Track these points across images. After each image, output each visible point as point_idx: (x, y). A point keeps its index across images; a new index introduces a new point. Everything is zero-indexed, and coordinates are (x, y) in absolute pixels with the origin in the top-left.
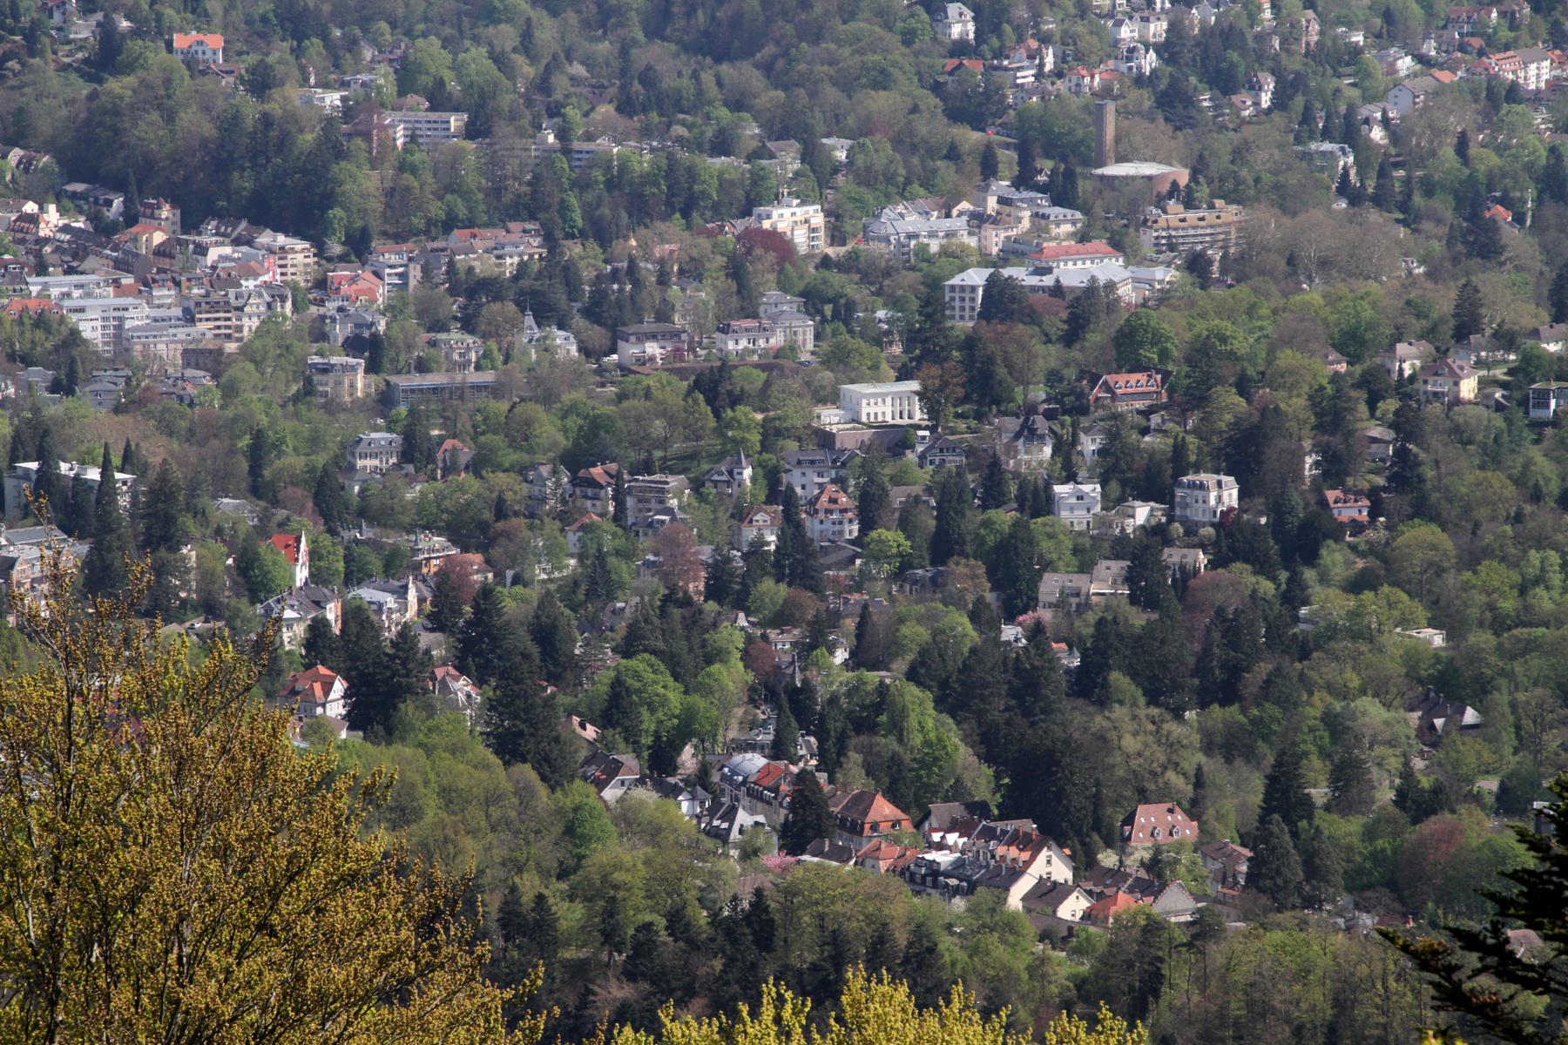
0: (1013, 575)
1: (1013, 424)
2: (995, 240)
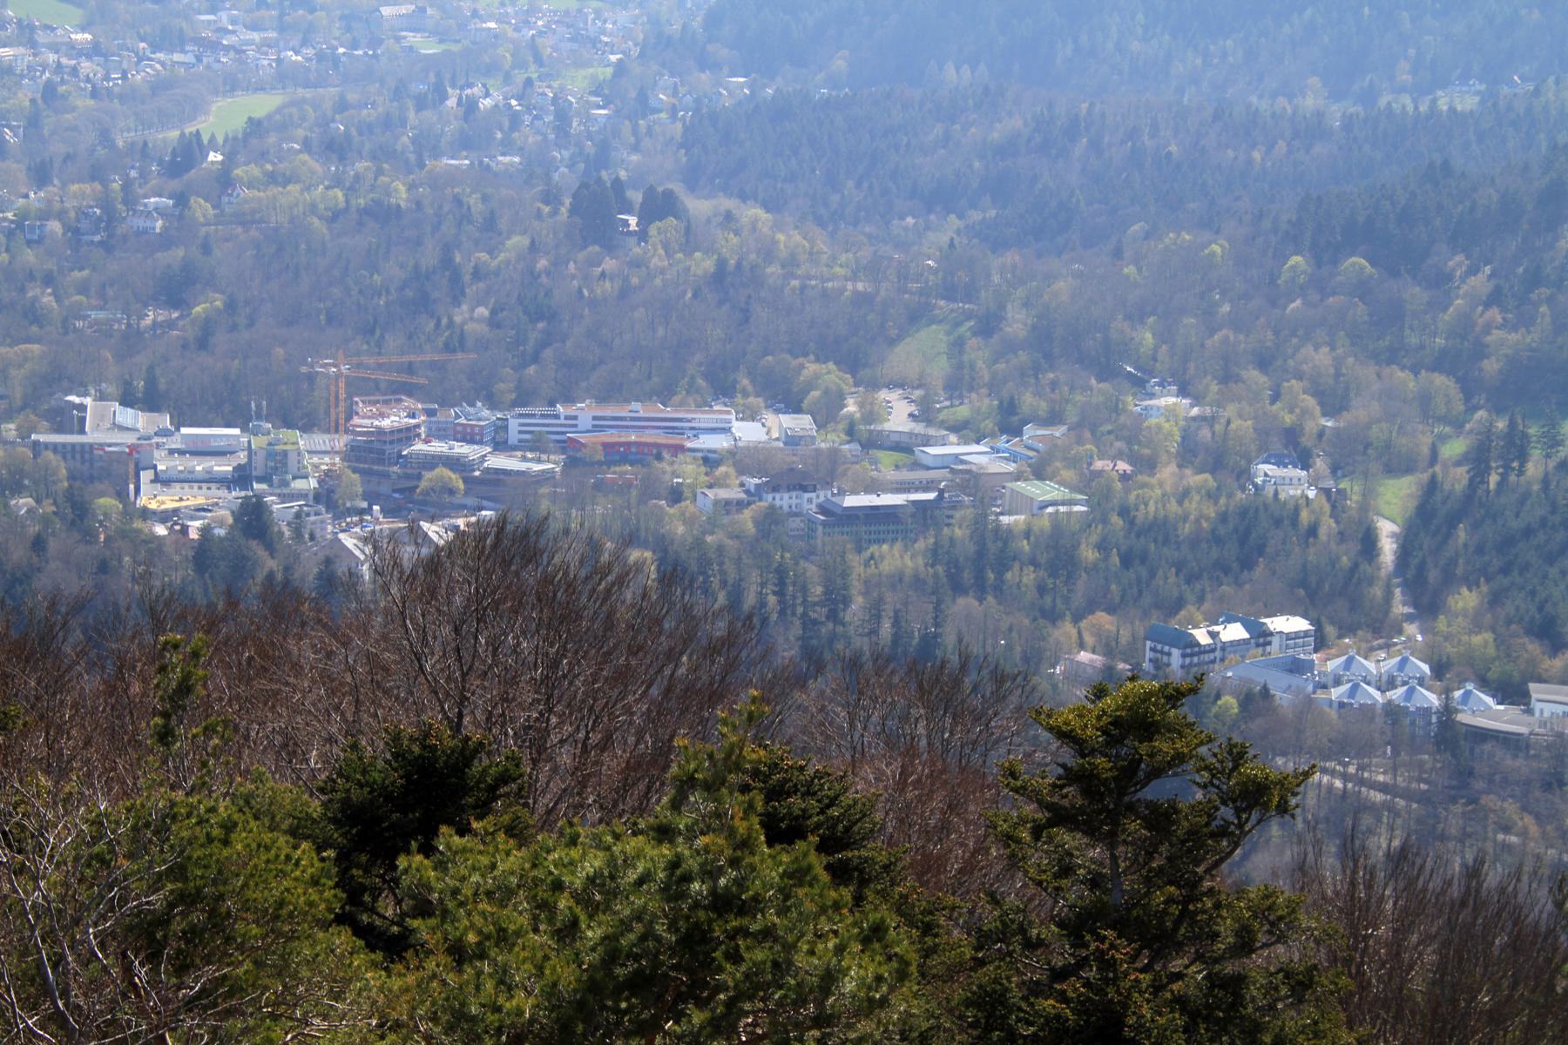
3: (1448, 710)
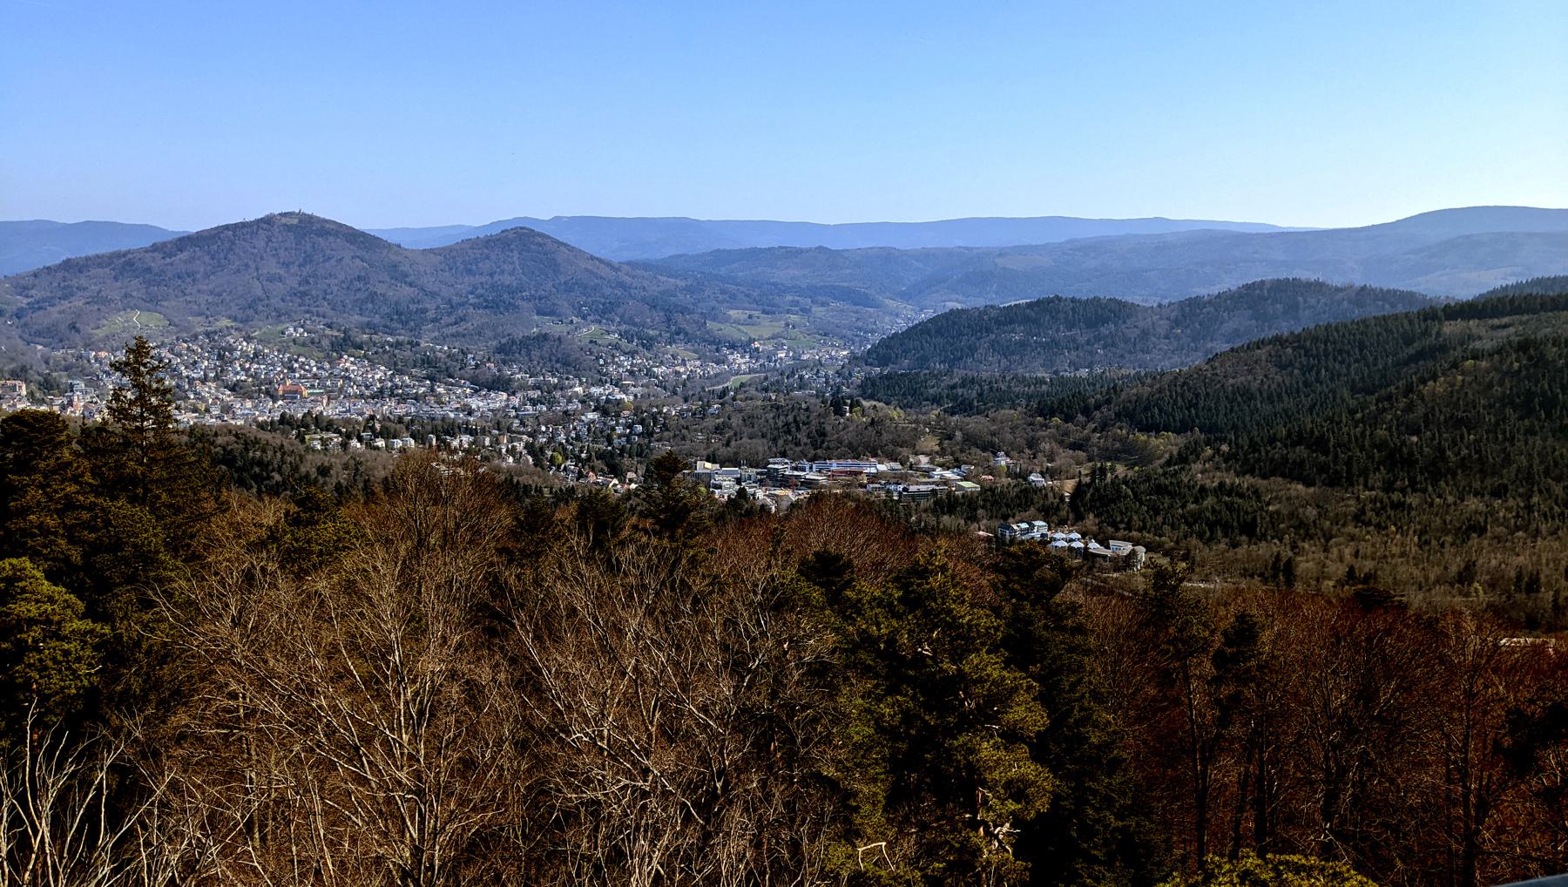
0: (610, 441)
3: (1086, 549)
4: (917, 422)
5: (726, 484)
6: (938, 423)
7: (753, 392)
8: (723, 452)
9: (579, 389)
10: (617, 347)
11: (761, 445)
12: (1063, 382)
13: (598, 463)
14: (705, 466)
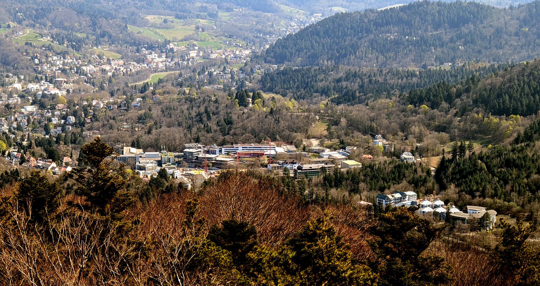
0: (47, 130)
1: (46, 111)
2: (43, 88)
3: (448, 213)
4: (308, 110)
5: (149, 165)
6: (326, 111)
7: (169, 87)
8: (146, 139)
9: (18, 86)
10: (50, 48)
11: (177, 133)
12: (430, 75)
13: (39, 150)
14: (129, 151)
